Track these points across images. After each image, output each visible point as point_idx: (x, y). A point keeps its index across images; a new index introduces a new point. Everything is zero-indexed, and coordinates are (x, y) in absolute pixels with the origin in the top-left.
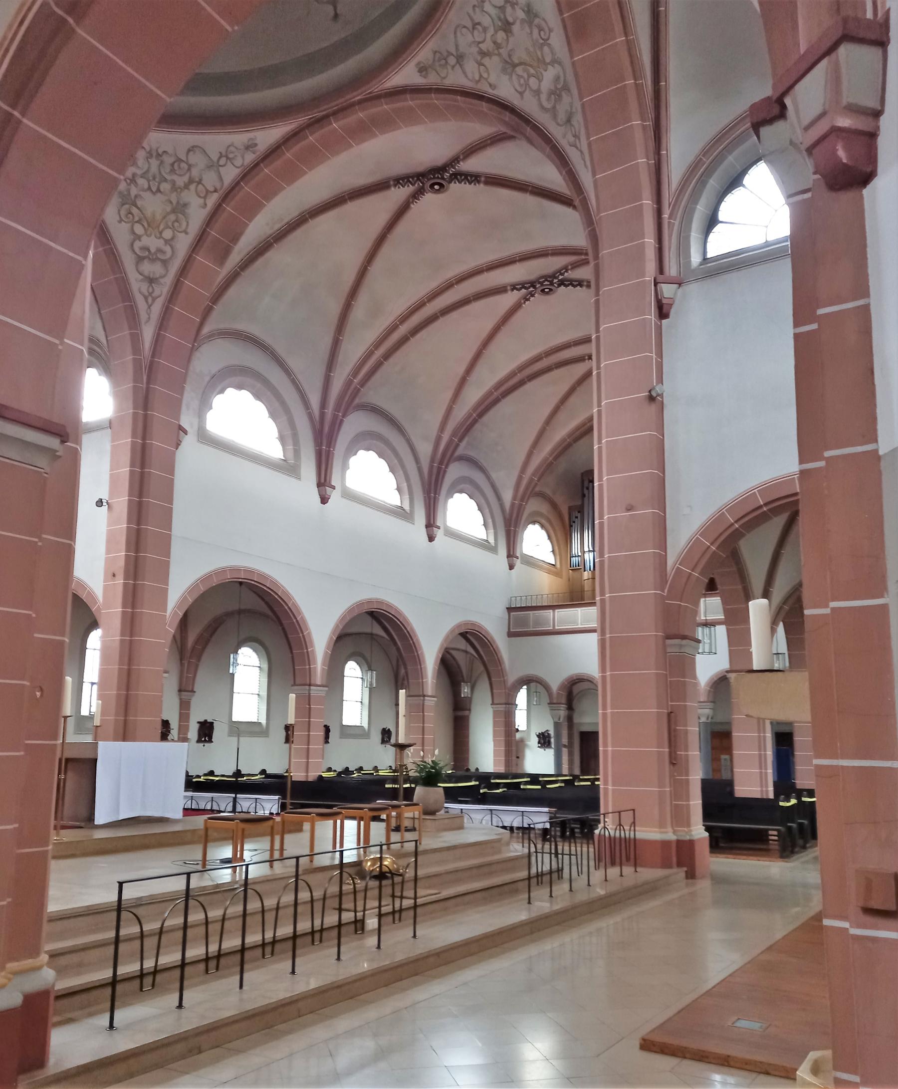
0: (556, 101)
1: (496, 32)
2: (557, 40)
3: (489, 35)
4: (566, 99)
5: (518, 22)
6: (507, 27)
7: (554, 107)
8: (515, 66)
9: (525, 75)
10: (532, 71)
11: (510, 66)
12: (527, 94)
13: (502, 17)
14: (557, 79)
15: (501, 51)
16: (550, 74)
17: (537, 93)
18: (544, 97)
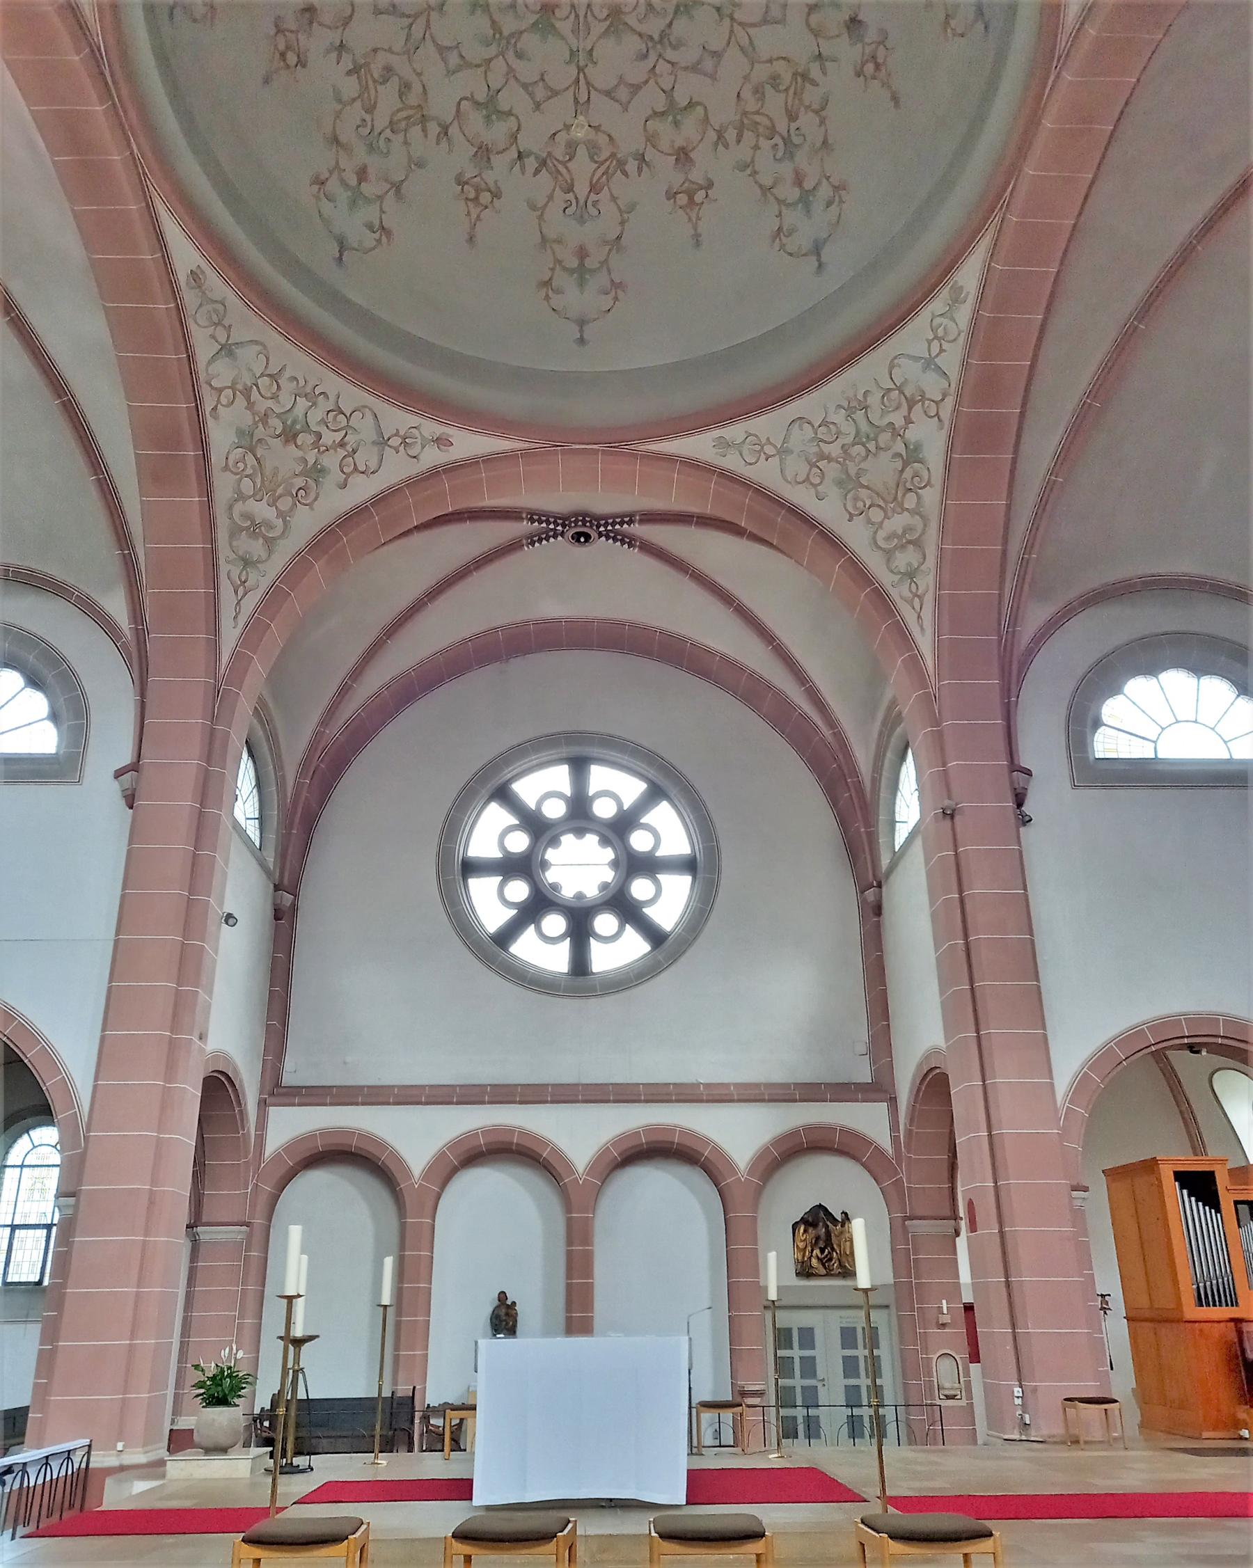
0: (247, 528)
1: (278, 416)
2: (307, 523)
3: (270, 403)
4: (256, 548)
5: (300, 454)
6: (289, 436)
7: (242, 529)
8: (252, 450)
9: (249, 471)
10: (258, 481)
11: (248, 442)
12: (230, 478)
13: (298, 427)
14: (271, 527)
15: (260, 425)
16: (263, 511)
17: (241, 497)
18: (239, 508)
